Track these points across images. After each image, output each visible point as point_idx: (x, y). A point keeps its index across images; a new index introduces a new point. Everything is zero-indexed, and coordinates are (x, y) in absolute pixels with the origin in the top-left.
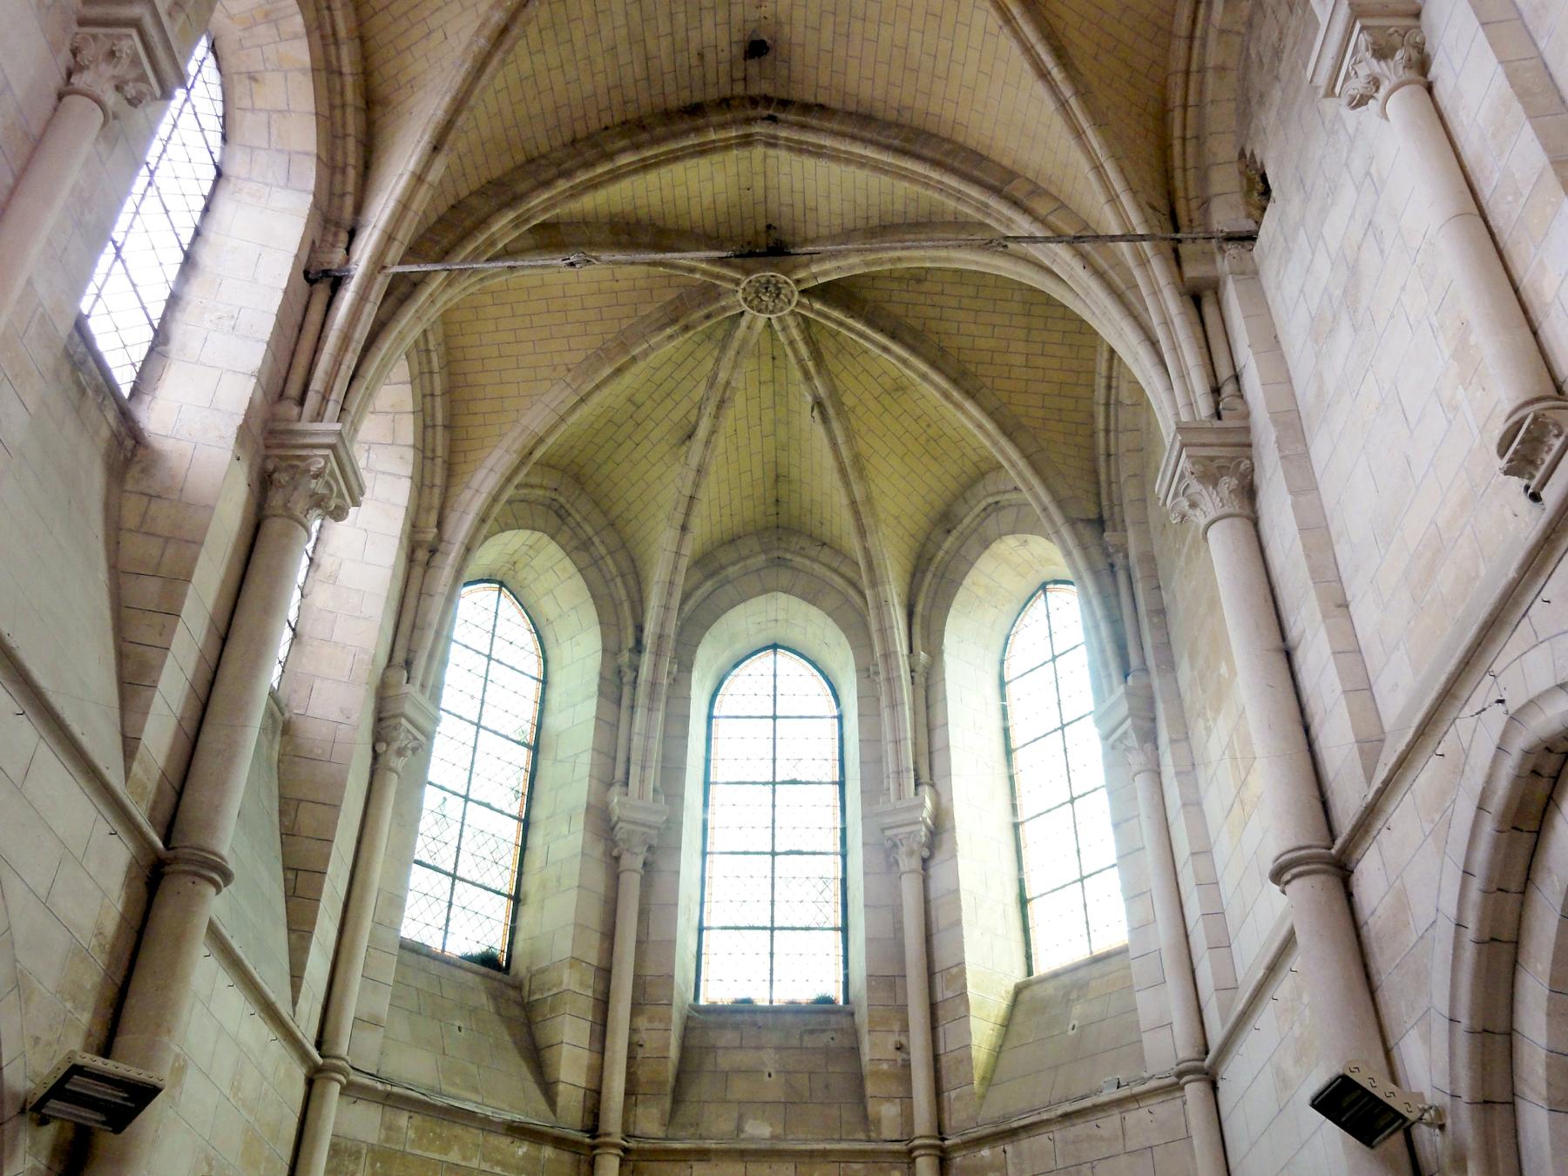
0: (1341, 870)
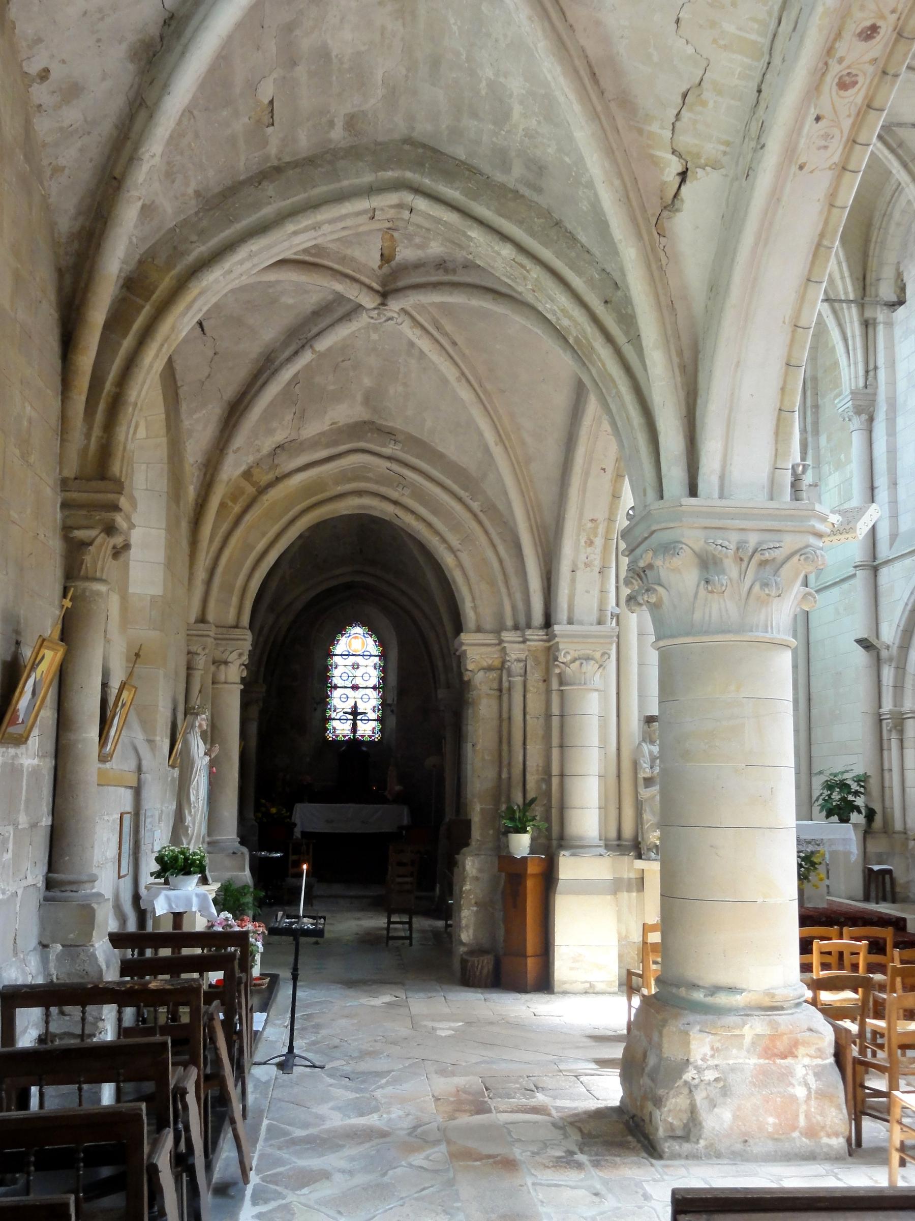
0: (875, 570)
